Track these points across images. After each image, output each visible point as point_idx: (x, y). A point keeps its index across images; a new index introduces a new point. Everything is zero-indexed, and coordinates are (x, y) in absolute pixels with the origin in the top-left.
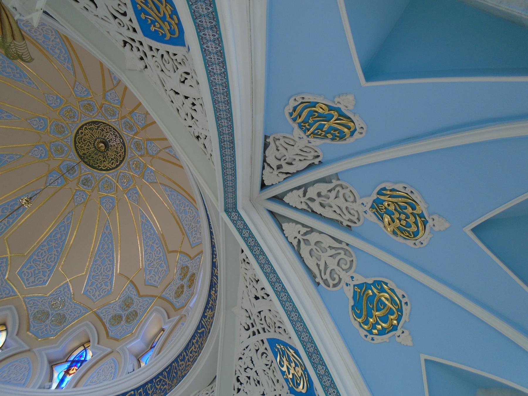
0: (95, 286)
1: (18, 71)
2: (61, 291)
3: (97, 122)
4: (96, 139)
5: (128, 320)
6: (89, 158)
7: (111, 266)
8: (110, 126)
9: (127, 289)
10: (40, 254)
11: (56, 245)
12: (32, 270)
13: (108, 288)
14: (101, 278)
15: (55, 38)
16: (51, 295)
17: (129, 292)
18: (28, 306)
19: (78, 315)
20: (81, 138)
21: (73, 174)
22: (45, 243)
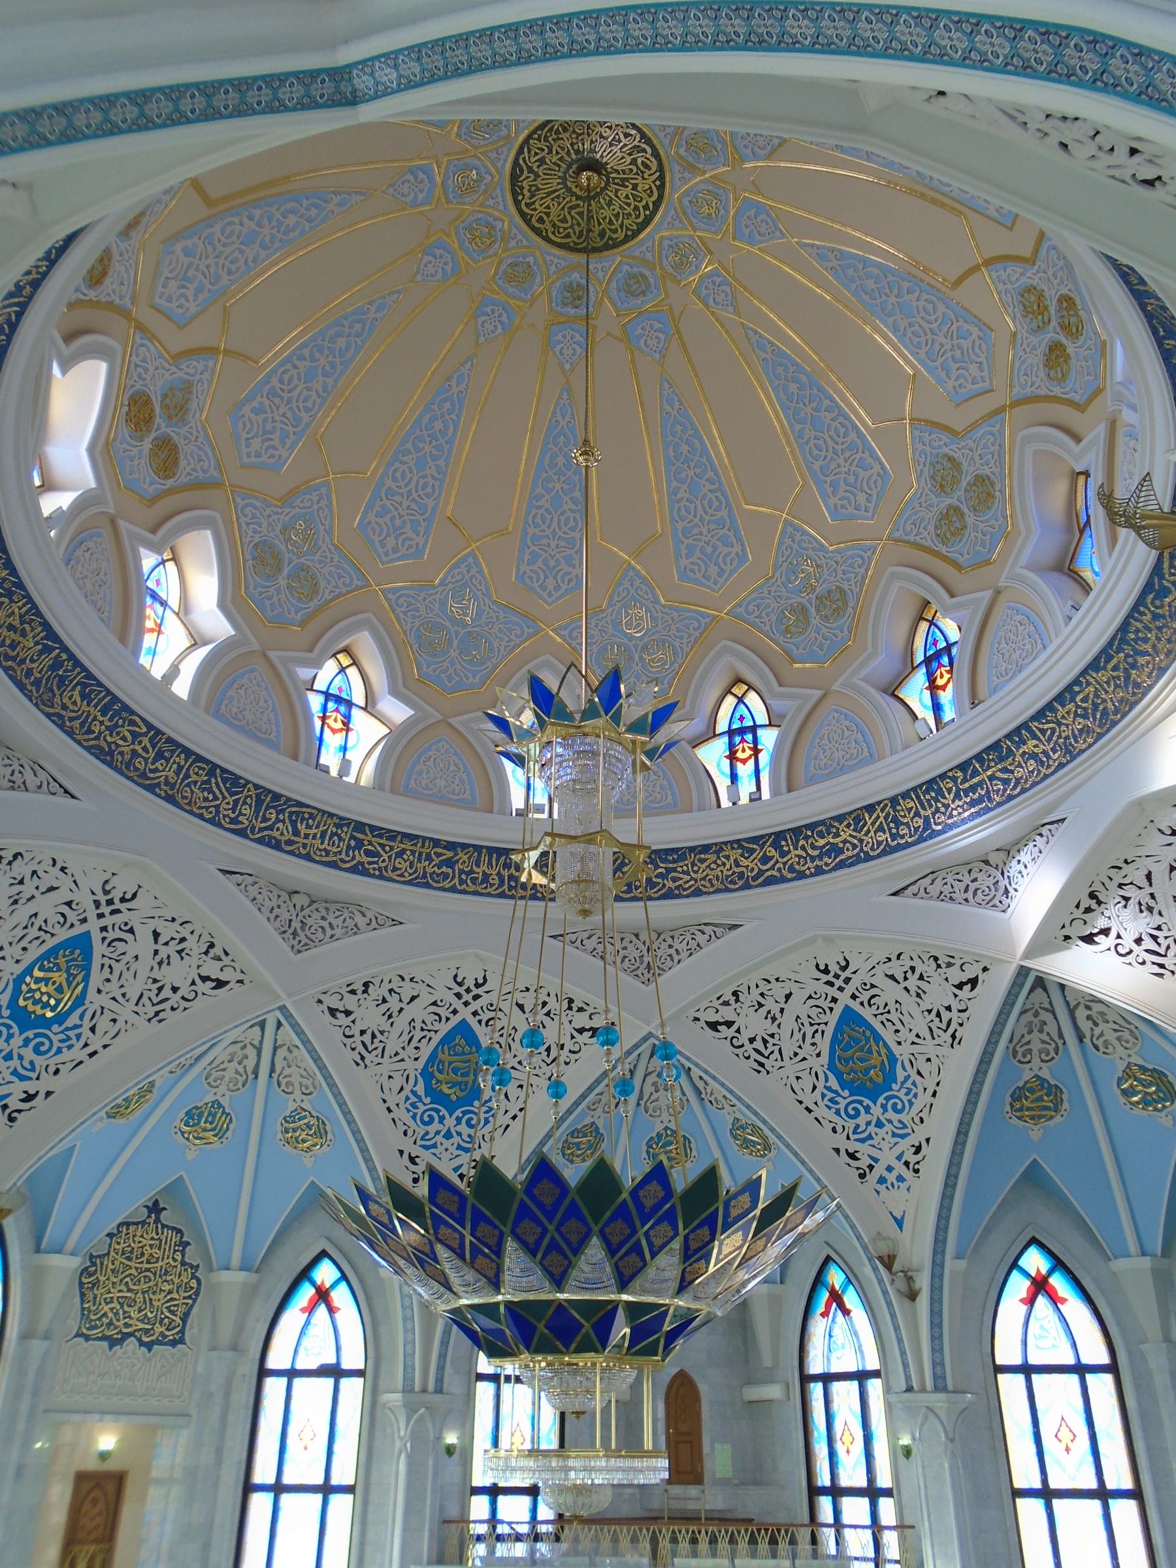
0: (954, 366)
1: (346, 323)
2: (923, 452)
3: (513, 169)
4: (566, 186)
5: (1073, 329)
6: (617, 224)
7: (924, 296)
8: (530, 137)
9: (1001, 286)
10: (815, 452)
11: (814, 405)
12: (843, 487)
13: (974, 336)
14: (943, 340)
15: (251, 218)
16: (918, 479)
17: (1009, 286)
18: (911, 538)
19: (997, 447)
20: (554, 226)
21: (648, 286)
22: (798, 427)
